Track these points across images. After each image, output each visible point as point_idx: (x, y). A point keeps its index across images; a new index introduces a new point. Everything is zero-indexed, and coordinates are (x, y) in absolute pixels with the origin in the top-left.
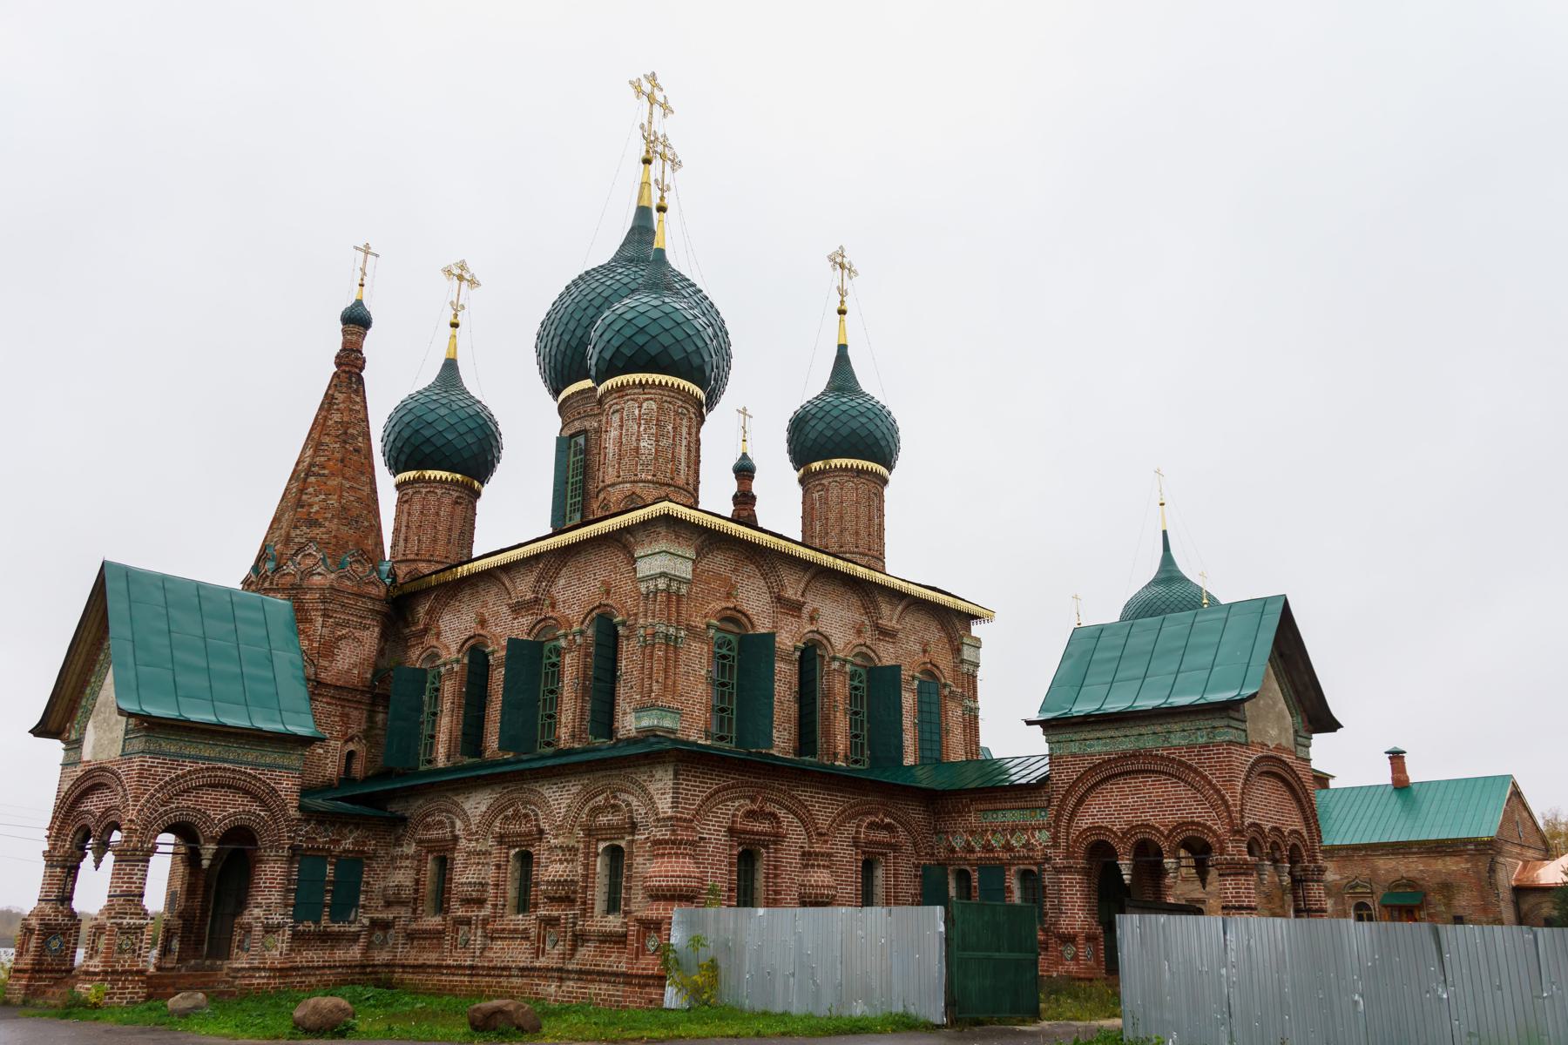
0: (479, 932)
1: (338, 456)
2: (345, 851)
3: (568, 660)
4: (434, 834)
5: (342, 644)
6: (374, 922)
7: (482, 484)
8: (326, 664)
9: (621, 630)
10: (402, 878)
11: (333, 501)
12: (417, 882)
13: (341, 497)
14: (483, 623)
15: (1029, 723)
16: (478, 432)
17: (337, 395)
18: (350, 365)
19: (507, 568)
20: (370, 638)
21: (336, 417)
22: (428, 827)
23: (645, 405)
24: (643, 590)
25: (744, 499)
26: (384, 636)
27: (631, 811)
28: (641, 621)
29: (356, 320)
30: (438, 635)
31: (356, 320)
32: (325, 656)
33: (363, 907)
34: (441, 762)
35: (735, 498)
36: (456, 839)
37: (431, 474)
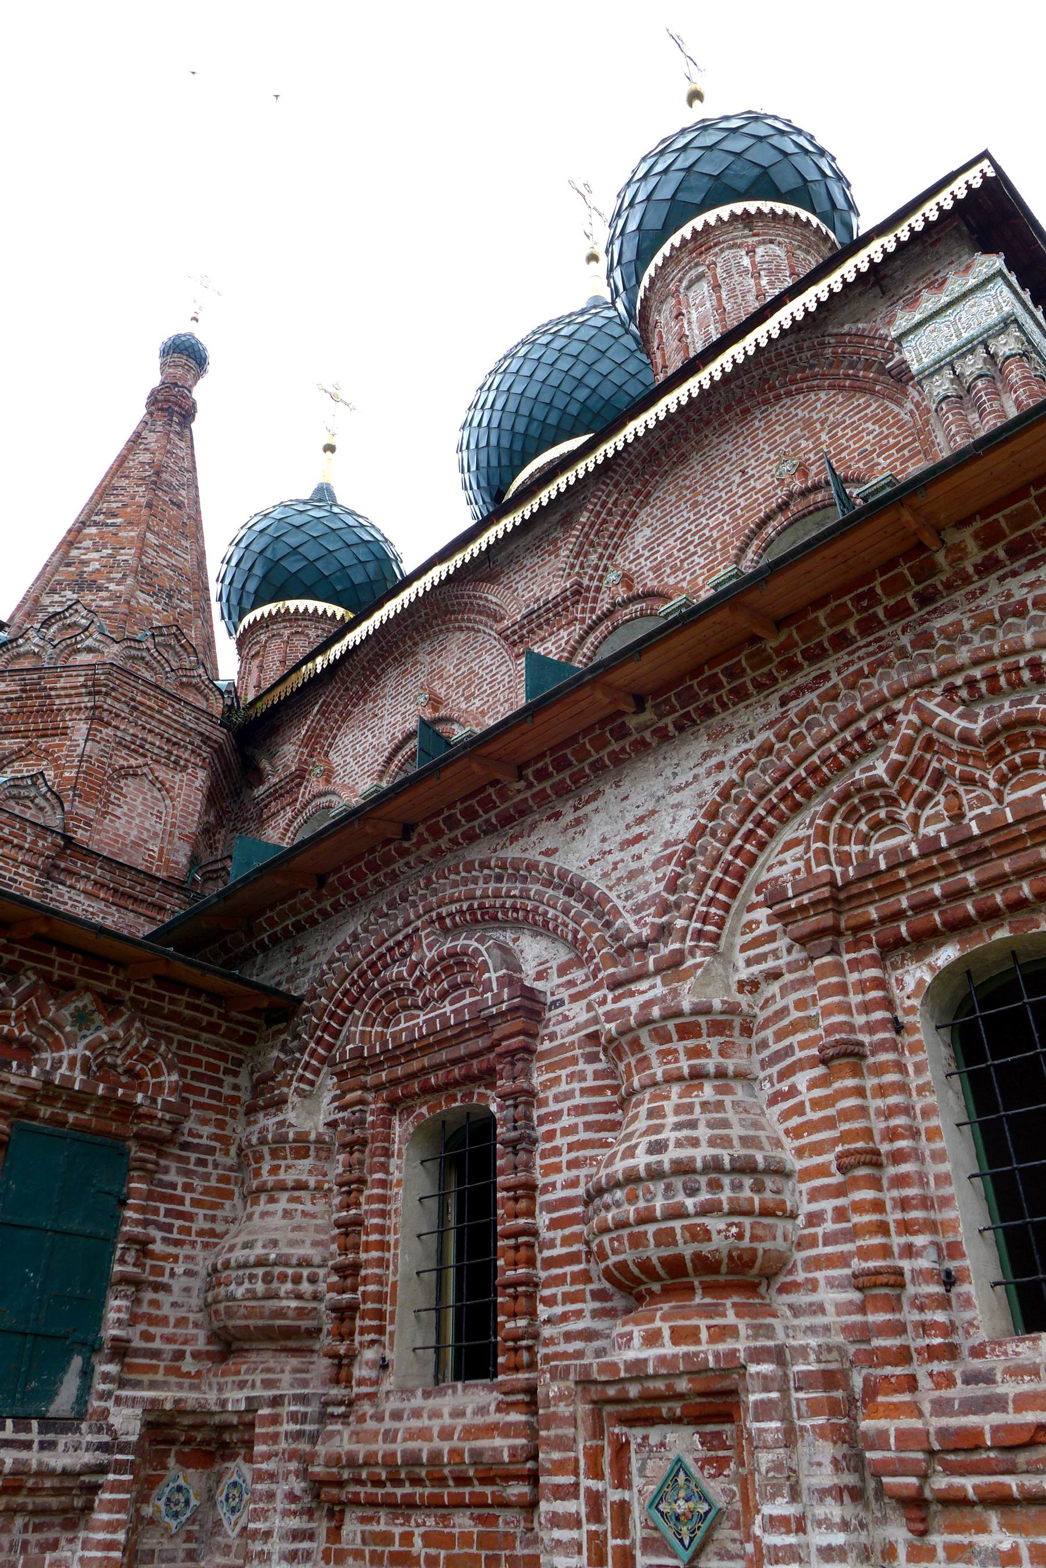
0: (819, 1463)
2: (49, 1091)
4: (416, 1023)
5: (129, 786)
6: (160, 1428)
8: (91, 813)
10: (284, 1231)
11: (128, 555)
12: (350, 1228)
13: (141, 552)
16: (373, 547)
18: (172, 407)
20: (190, 787)
21: (146, 457)
22: (395, 1000)
23: (760, 250)
26: (213, 797)
29: (186, 356)
30: (328, 775)
31: (186, 356)
32: (86, 798)
33: (120, 1351)
36: (531, 1007)
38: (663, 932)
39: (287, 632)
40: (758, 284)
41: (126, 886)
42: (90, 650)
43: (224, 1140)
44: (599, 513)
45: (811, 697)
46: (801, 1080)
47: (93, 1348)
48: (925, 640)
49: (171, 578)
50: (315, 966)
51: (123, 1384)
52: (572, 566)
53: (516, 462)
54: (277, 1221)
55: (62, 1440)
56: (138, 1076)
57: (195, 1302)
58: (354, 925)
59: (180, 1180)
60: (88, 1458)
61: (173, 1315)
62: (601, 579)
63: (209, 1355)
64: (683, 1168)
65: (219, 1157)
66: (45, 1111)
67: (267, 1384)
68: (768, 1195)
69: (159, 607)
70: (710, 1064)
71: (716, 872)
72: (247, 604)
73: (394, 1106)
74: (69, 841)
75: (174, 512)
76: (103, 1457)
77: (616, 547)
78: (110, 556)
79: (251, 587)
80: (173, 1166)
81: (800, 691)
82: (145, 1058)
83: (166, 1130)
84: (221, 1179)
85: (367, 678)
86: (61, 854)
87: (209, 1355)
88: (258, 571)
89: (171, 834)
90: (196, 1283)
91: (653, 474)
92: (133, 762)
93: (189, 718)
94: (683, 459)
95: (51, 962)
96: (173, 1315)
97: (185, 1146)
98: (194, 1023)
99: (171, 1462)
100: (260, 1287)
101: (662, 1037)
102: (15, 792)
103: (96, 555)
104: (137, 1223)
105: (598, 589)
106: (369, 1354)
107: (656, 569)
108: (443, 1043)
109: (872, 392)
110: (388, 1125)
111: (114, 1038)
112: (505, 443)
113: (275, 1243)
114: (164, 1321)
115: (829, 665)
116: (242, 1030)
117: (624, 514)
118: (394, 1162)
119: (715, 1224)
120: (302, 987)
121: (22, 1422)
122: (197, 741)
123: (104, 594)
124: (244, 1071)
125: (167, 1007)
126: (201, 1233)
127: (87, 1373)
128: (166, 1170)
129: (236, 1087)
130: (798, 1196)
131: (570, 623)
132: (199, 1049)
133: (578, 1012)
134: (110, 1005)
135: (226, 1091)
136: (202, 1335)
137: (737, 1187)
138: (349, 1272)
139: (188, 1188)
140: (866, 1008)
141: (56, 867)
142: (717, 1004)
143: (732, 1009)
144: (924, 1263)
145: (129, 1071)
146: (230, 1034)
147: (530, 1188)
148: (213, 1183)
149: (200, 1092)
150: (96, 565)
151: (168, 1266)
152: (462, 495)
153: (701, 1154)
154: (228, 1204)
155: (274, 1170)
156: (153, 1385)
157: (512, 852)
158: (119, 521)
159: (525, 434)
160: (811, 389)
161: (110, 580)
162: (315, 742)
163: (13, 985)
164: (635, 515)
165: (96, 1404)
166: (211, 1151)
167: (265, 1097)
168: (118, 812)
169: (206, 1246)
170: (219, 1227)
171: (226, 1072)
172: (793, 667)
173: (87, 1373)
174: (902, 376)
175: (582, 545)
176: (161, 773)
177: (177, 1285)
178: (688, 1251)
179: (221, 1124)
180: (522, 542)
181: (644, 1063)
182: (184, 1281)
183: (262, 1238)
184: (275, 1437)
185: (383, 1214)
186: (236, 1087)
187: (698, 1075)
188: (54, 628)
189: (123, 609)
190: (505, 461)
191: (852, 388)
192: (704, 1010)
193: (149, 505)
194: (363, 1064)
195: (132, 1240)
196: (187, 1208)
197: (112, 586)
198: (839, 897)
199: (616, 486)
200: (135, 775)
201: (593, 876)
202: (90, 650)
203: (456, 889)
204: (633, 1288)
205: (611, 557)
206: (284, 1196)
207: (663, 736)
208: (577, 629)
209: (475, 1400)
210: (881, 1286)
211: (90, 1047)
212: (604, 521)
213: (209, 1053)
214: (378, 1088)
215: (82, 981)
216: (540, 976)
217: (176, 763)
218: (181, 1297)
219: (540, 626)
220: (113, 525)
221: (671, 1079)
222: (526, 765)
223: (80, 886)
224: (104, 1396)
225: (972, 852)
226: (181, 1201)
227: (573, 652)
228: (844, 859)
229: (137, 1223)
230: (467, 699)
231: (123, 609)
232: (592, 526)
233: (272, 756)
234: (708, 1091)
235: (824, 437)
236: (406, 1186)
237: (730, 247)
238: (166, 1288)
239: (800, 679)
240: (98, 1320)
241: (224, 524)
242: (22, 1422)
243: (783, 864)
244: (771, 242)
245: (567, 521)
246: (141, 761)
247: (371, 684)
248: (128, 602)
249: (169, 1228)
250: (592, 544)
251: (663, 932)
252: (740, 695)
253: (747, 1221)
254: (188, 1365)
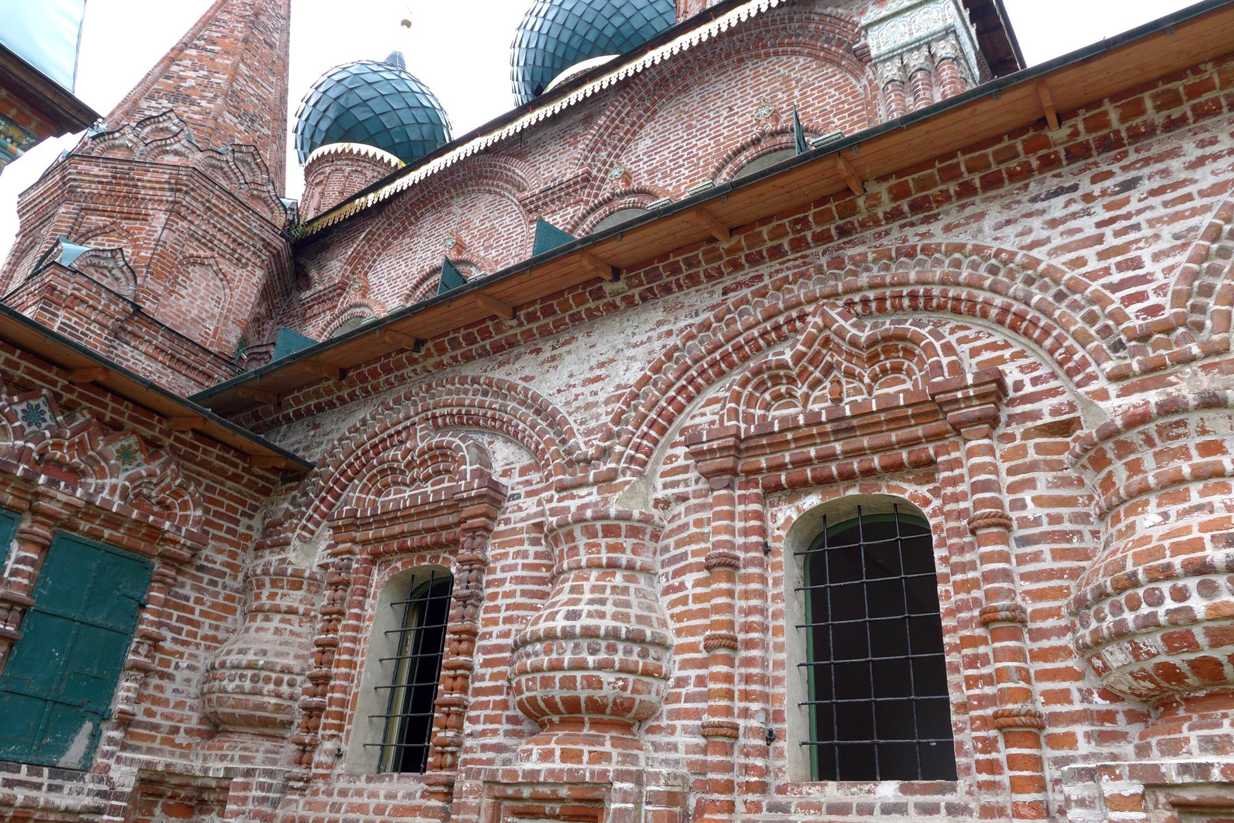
1: (241, 36)
2: (90, 510)
5: (196, 272)
8: (160, 290)
10: (273, 645)
11: (221, 79)
12: (326, 648)
13: (233, 79)
20: (248, 282)
22: (389, 475)
26: (267, 293)
30: (365, 291)
32: (158, 276)
33: (125, 722)
36: (494, 496)
38: (604, 453)
39: (348, 169)
41: (182, 354)
42: (176, 153)
43: (234, 568)
44: (613, 120)
45: (746, 292)
46: (689, 579)
47: (103, 717)
48: (838, 263)
49: (255, 106)
50: (327, 441)
51: (124, 747)
52: (586, 158)
53: (557, 66)
54: (269, 636)
55: (68, 785)
56: (168, 508)
57: (193, 690)
58: (365, 413)
59: (193, 595)
60: (88, 801)
61: (173, 698)
62: (607, 172)
63: (199, 733)
64: (590, 634)
65: (227, 580)
66: (84, 526)
67: (243, 759)
68: (650, 660)
70: (623, 559)
71: (651, 414)
72: (318, 140)
73: (375, 558)
74: (138, 309)
75: (266, 50)
76: (101, 802)
77: (623, 149)
78: (205, 77)
79: (324, 125)
80: (189, 582)
81: (739, 285)
82: (176, 494)
83: (186, 554)
84: (227, 598)
85: (408, 218)
86: (129, 319)
87: (199, 733)
88: (332, 114)
89: (226, 317)
90: (196, 677)
91: (662, 97)
92: (202, 253)
93: (255, 225)
94: (686, 89)
95: (105, 406)
96: (173, 698)
97: (201, 568)
98: (221, 472)
99: (158, 811)
100: (248, 685)
101: (590, 533)
102: (95, 261)
103: (194, 74)
104: (153, 623)
105: (603, 180)
106: (328, 745)
107: (650, 173)
108: (421, 515)
109: (839, 65)
110: (369, 573)
111: (151, 474)
112: (550, 48)
113: (264, 653)
114: (166, 703)
115: (764, 269)
116: (261, 483)
117: (633, 124)
118: (369, 601)
119: (607, 677)
120: (314, 456)
121: (35, 768)
122: (259, 245)
123: (196, 108)
124: (258, 516)
125: (200, 456)
126: (205, 638)
127: (95, 736)
128: (183, 586)
129: (250, 528)
130: (672, 665)
131: (576, 203)
132: (222, 493)
133: (530, 506)
134: (152, 447)
135: (241, 529)
136: (195, 716)
137: (628, 652)
138: (320, 681)
139: (198, 601)
140: (746, 532)
141: (124, 329)
142: (636, 514)
143: (647, 519)
144: (754, 723)
145: (161, 503)
146: (250, 485)
147: (473, 634)
148: (221, 600)
149: (220, 527)
150: (191, 83)
151: (174, 660)
152: (509, 84)
153: (605, 624)
154: (230, 618)
155: (272, 596)
156: (150, 751)
157: (498, 374)
158: (217, 48)
159: (567, 44)
160: (794, 53)
161: (203, 98)
162: (357, 261)
163: (70, 419)
164: (641, 127)
165: (100, 760)
166: (223, 575)
167: (273, 538)
168: (183, 292)
169: (208, 648)
170: (221, 635)
171: (243, 514)
172: (737, 266)
173: (95, 736)
174: (863, 57)
175: (596, 142)
176: (225, 266)
177: (179, 676)
178: (583, 694)
179: (233, 555)
180: (550, 131)
181: (574, 551)
182: (187, 674)
183: (254, 647)
184: (244, 800)
185: (354, 640)
186: (250, 528)
187: (613, 565)
188: (148, 129)
189: (211, 124)
190: (548, 63)
191: (825, 58)
192: (626, 517)
193: (245, 41)
194: (355, 522)
195: (147, 636)
196: (196, 617)
197: (204, 103)
198: (740, 446)
199: (631, 100)
200: (202, 264)
201: (558, 402)
202: (176, 153)
203: (450, 396)
204: (538, 717)
205: (617, 156)
206: (278, 617)
207: (630, 302)
208: (582, 209)
209: (407, 786)
210: (721, 736)
211: (128, 479)
212: (617, 127)
213: (231, 498)
214: (364, 543)
215: (130, 425)
216: (505, 473)
217: (239, 260)
218: (182, 685)
219: (552, 201)
221: (592, 565)
222: (520, 307)
223: (143, 348)
224: (107, 755)
225: (843, 428)
226: (192, 611)
227: (576, 226)
228: (749, 419)
229: (153, 623)
231: (211, 124)
232: (607, 128)
233: (321, 268)
234: (619, 579)
235: (796, 93)
236: (377, 622)
238: (170, 677)
239: (740, 277)
240: (110, 696)
242: (35, 768)
243: (703, 415)
245: (588, 121)
246: (209, 253)
247: (411, 224)
248: (215, 119)
249: (179, 631)
250: (604, 143)
251: (604, 453)
252: (694, 280)
253: (631, 678)
254: (181, 738)
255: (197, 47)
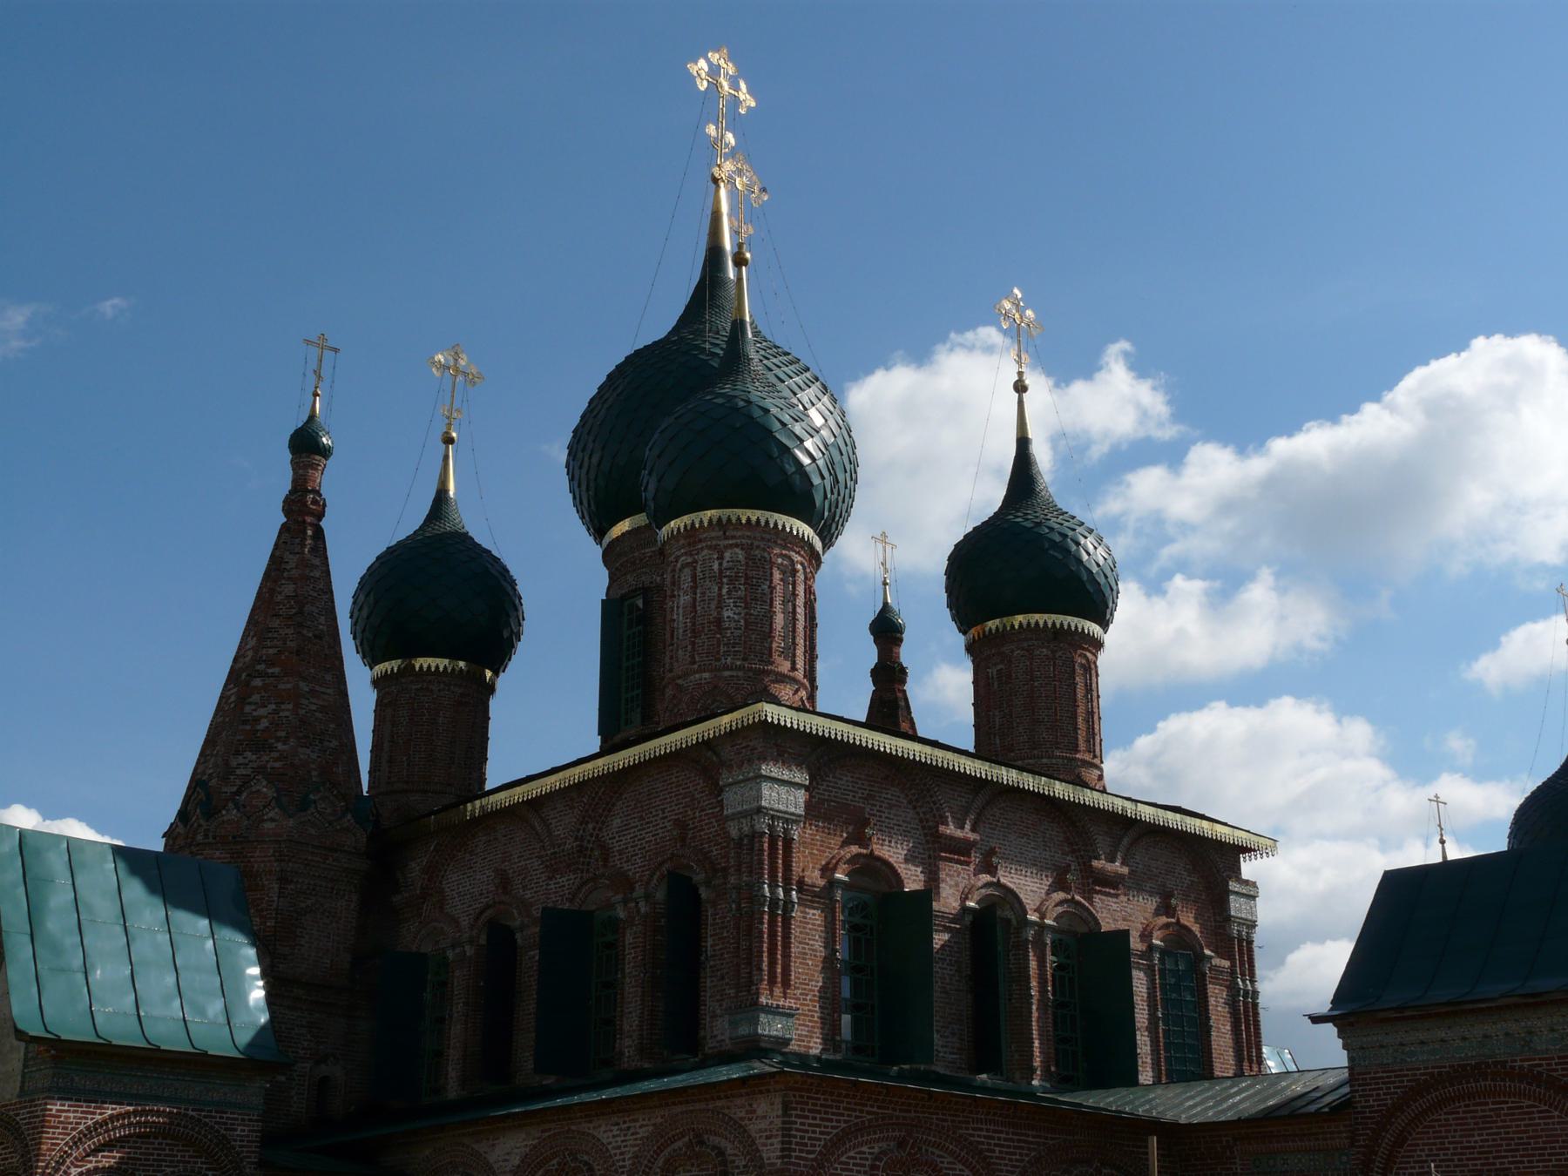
3: (629, 939)
7: (496, 673)
9: (704, 893)
14: (504, 883)
15: (1316, 1019)
17: (288, 556)
18: (303, 513)
19: (535, 804)
21: (289, 589)
23: (727, 555)
24: (734, 833)
25: (889, 678)
27: (724, 1163)
28: (732, 880)
34: (453, 1091)
35: (875, 673)
37: (423, 663)
40: (720, 595)
42: (272, 820)
69: (314, 756)
78: (276, 712)
103: (262, 712)
123: (275, 755)
150: (264, 723)
158: (276, 670)
161: (278, 739)
188: (244, 795)
202: (272, 820)
220: (272, 675)
230: (525, 888)
237: (709, 547)
241: (349, 561)
244: (737, 546)
255: (261, 675)
